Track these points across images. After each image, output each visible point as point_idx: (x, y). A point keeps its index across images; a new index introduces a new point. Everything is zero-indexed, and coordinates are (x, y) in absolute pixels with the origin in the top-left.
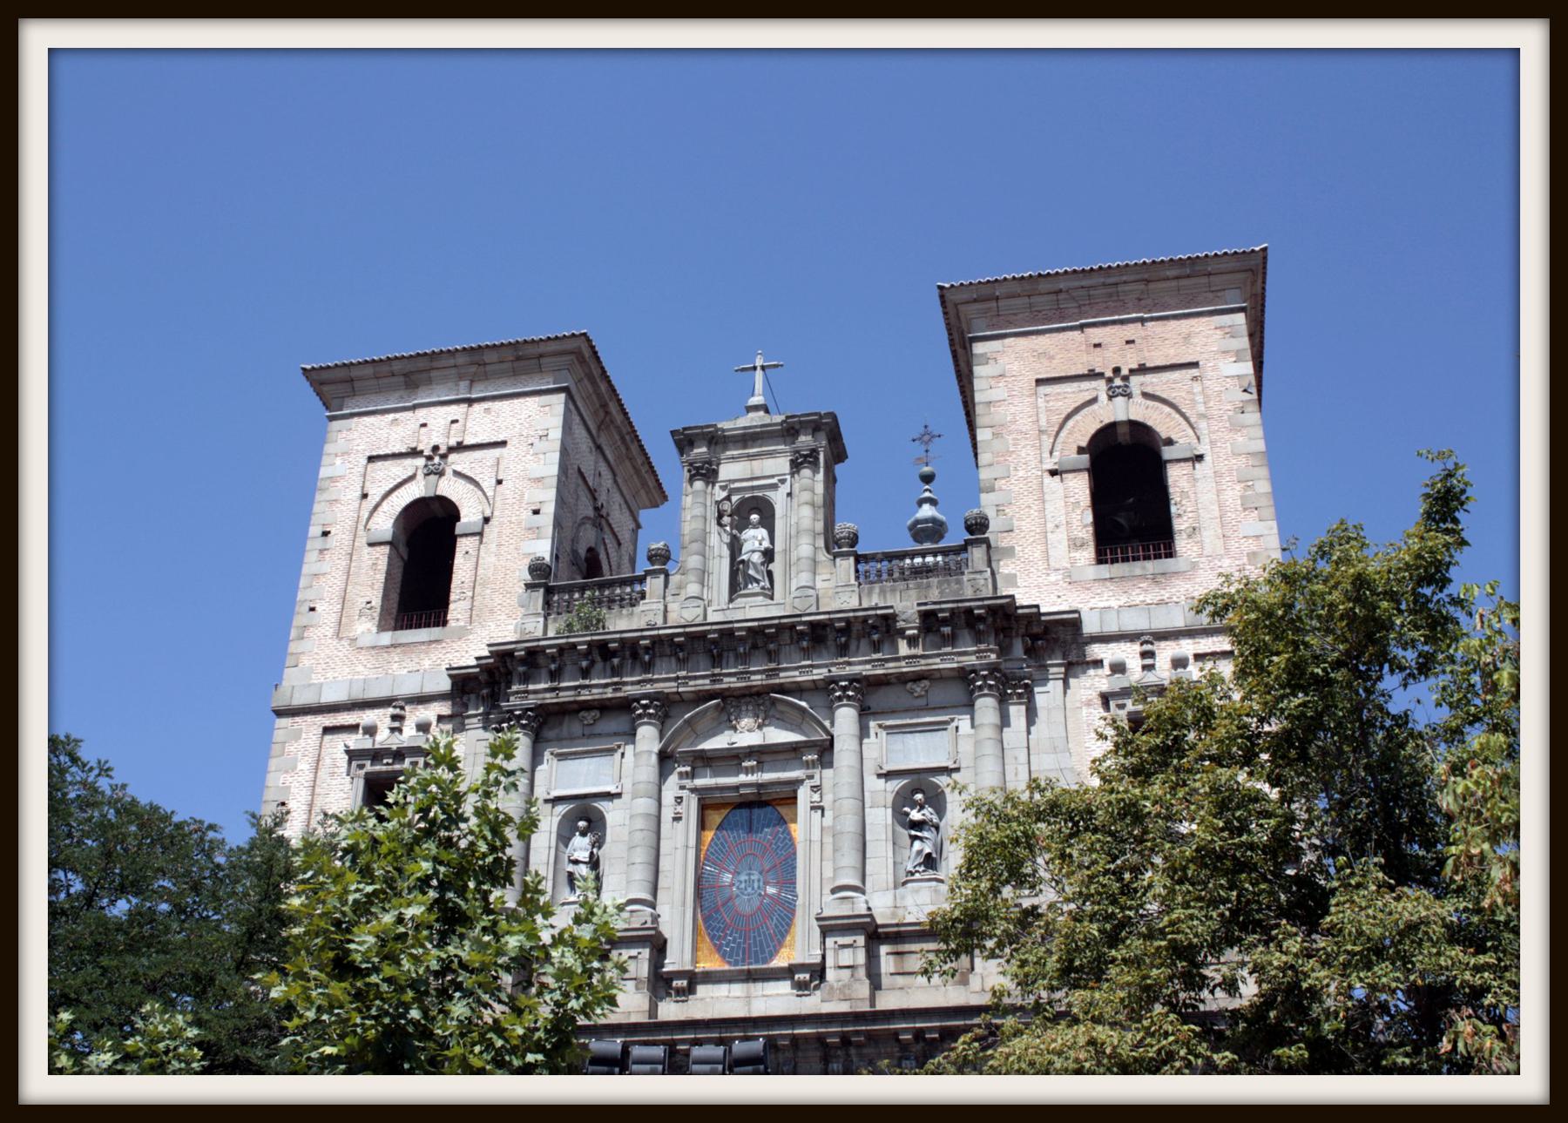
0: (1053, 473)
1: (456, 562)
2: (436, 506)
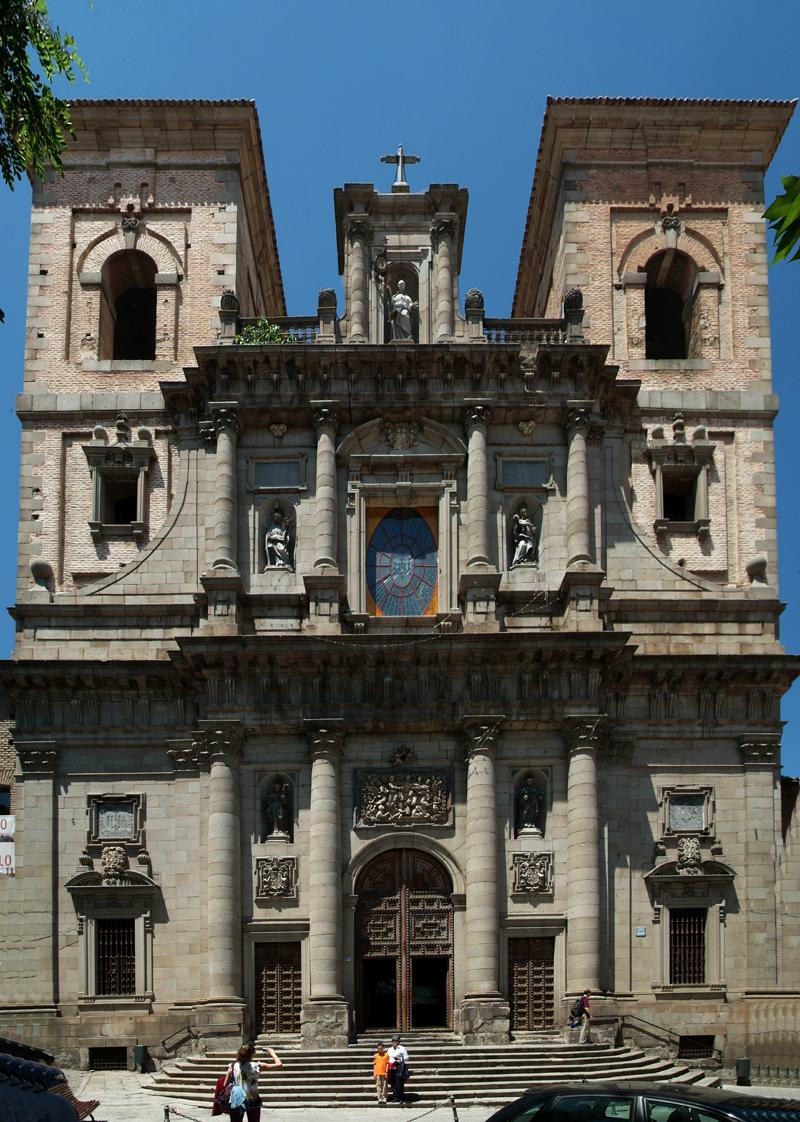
0: (618, 287)
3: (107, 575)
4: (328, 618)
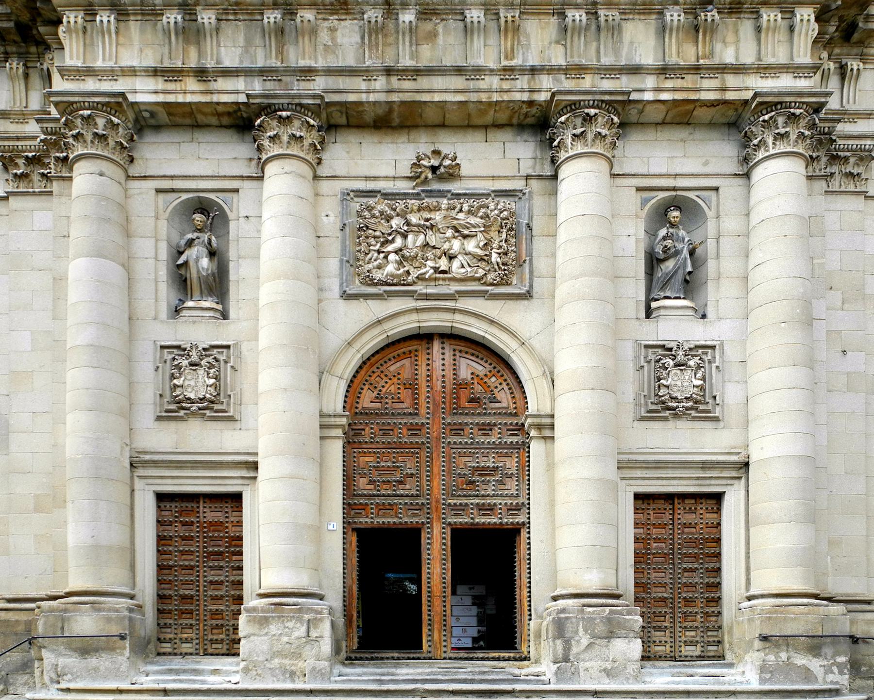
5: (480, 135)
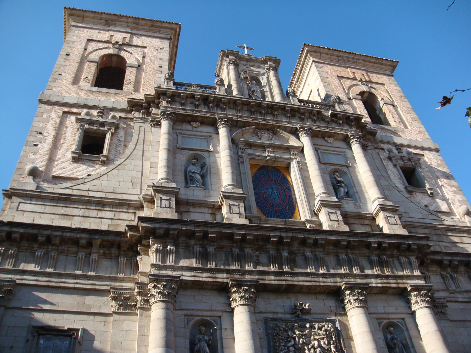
1: (126, 73)
2: (114, 59)
3: (77, 179)
4: (238, 215)
5: (313, 296)
